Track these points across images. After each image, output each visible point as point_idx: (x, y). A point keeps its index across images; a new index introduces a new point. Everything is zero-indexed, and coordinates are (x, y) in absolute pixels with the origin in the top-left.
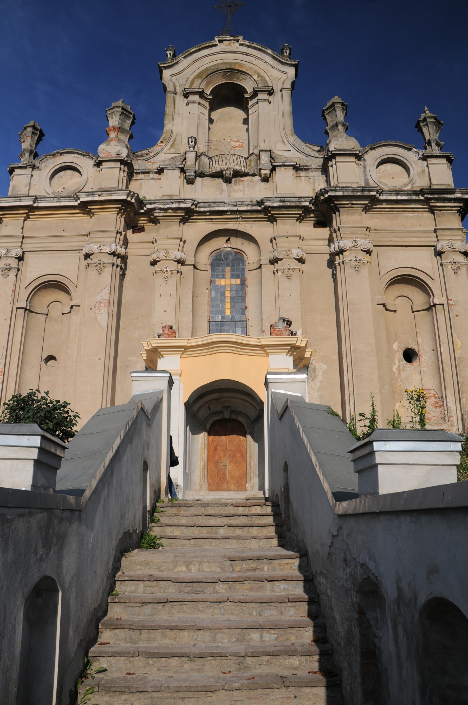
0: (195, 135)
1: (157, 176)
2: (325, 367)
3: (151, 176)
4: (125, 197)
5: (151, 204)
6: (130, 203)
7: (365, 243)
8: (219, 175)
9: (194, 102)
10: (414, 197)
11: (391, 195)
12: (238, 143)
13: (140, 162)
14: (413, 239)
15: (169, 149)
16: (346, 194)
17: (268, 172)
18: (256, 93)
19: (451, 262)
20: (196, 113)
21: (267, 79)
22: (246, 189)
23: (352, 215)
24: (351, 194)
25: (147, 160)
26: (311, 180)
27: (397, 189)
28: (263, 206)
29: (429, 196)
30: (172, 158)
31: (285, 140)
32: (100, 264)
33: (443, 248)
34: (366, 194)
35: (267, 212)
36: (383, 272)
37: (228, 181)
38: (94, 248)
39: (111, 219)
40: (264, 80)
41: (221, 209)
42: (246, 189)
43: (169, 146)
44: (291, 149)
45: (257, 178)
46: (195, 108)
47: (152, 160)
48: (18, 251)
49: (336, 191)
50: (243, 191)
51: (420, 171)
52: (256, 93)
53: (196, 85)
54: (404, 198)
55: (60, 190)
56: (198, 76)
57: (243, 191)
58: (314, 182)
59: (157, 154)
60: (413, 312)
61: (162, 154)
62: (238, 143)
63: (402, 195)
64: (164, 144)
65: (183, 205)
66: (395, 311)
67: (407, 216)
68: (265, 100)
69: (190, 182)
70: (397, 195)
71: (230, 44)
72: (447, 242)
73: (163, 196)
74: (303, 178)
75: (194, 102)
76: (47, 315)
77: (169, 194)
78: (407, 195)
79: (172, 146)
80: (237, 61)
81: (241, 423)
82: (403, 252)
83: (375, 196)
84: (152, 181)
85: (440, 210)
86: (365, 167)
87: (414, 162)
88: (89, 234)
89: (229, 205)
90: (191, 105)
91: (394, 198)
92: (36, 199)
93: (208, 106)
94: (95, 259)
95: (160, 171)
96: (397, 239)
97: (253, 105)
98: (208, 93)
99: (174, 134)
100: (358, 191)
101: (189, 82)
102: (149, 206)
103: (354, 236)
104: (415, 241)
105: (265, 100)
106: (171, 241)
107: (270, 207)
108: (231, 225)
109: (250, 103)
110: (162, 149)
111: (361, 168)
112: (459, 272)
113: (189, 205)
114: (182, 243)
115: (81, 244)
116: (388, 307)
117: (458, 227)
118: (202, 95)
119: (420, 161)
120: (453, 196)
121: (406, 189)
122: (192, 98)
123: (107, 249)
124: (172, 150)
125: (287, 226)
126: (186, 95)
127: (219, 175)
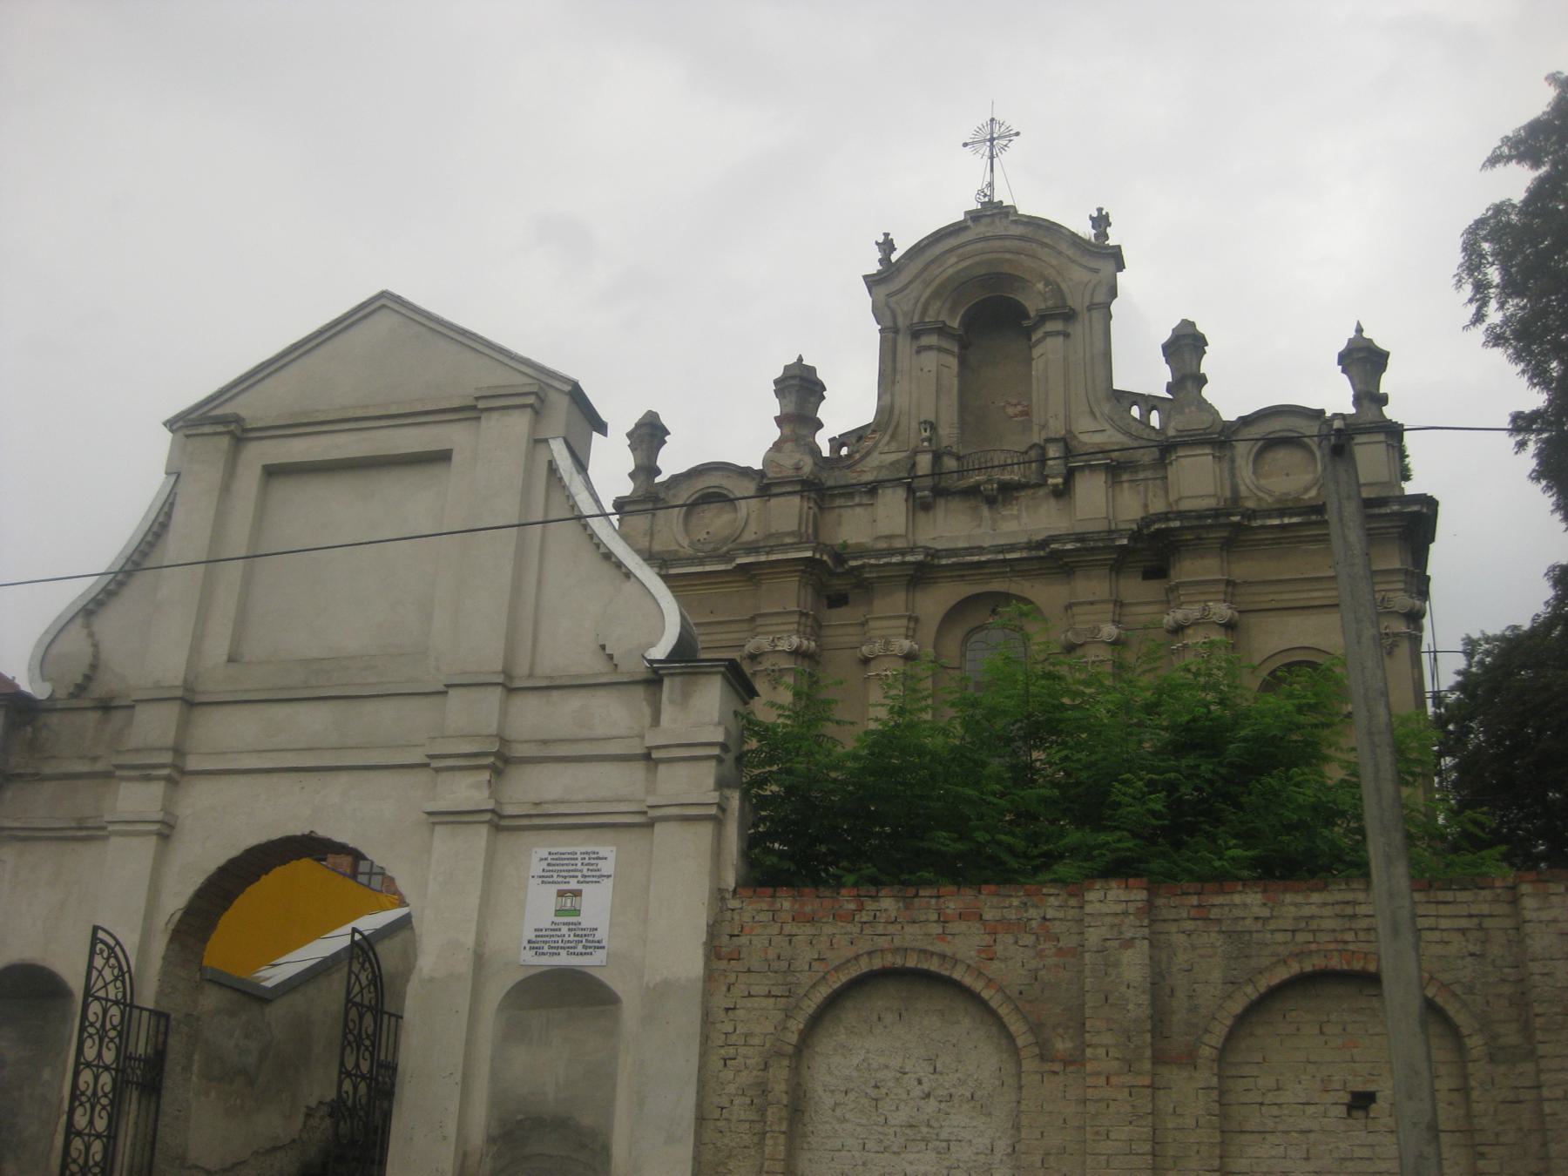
0: (932, 418)
1: (865, 500)
3: (857, 500)
4: (809, 554)
5: (855, 558)
7: (1221, 611)
8: (972, 492)
9: (930, 348)
10: (1314, 518)
12: (1020, 408)
13: (837, 473)
14: (1316, 594)
15: (888, 443)
17: (1060, 480)
18: (1044, 318)
20: (934, 369)
21: (1064, 286)
22: (1024, 514)
24: (1195, 523)
25: (849, 467)
26: (1141, 488)
30: (892, 464)
31: (1096, 410)
34: (1222, 520)
35: (1054, 560)
37: (991, 501)
38: (763, 642)
39: (788, 595)
40: (1058, 292)
41: (976, 558)
42: (1024, 514)
43: (887, 438)
44: (1106, 426)
45: (1042, 492)
46: (930, 360)
47: (859, 468)
49: (1168, 520)
50: (1018, 517)
52: (1044, 318)
53: (931, 312)
54: (1295, 520)
55: (702, 536)
56: (936, 294)
57: (1018, 517)
58: (1146, 491)
59: (868, 454)
61: (875, 454)
62: (1020, 408)
63: (1291, 516)
64: (877, 436)
65: (909, 558)
68: (1058, 333)
69: (926, 507)
71: (993, 222)
73: (878, 538)
74: (1126, 485)
75: (930, 348)
77: (887, 533)
79: (893, 437)
80: (1008, 256)
83: (1238, 524)
84: (859, 510)
86: (1233, 460)
88: (753, 619)
89: (990, 552)
90: (924, 355)
91: (1276, 522)
93: (956, 350)
94: (766, 664)
95: (873, 489)
96: (1286, 596)
97: (1039, 341)
98: (955, 324)
99: (896, 412)
100: (1208, 517)
101: (919, 305)
102: (853, 563)
105: (1058, 333)
106: (893, 623)
108: (996, 586)
110: (876, 445)
111: (1226, 466)
113: (920, 557)
114: (912, 625)
115: (741, 635)
117: (1397, 564)
118: (942, 330)
120: (1383, 511)
122: (926, 340)
123: (783, 645)
124: (894, 446)
125: (1091, 586)
126: (916, 335)
127: (972, 492)
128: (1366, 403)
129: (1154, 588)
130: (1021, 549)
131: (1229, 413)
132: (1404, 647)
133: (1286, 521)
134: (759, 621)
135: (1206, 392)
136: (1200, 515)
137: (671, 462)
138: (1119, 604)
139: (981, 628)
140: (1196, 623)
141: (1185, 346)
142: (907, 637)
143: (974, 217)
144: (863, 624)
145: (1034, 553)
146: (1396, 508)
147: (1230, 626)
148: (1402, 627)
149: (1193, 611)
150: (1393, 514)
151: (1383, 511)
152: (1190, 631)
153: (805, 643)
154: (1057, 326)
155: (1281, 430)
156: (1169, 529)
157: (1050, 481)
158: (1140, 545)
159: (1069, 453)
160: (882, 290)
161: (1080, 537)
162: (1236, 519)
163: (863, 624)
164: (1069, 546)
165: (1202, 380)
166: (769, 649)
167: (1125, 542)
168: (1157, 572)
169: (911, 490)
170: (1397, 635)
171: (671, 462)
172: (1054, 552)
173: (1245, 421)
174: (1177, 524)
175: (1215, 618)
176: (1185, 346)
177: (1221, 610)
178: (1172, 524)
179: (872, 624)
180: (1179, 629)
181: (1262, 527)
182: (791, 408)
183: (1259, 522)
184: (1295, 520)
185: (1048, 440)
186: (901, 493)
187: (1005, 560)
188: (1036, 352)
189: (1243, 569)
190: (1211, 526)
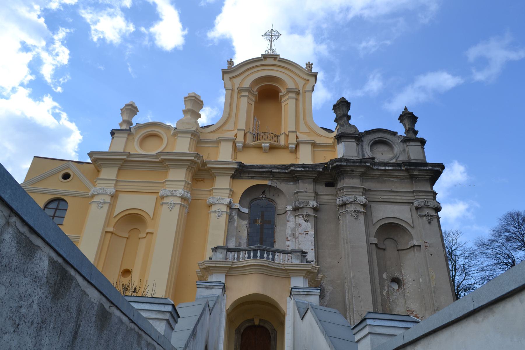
2: (332, 288)
4: (193, 158)
6: (196, 163)
11: (381, 166)
16: (348, 164)
17: (294, 146)
19: (425, 215)
23: (353, 179)
24: (352, 164)
27: (385, 161)
28: (289, 170)
29: (409, 167)
32: (171, 203)
33: (419, 205)
34: (363, 164)
36: (375, 221)
48: (112, 190)
49: (342, 162)
51: (401, 150)
54: (390, 168)
60: (398, 250)
63: (389, 167)
66: (384, 249)
67: (393, 181)
70: (385, 166)
72: (423, 200)
76: (127, 238)
78: (392, 166)
81: (267, 330)
82: (389, 207)
83: (369, 166)
85: (417, 178)
86: (362, 146)
87: (397, 143)
91: (383, 168)
92: (129, 155)
103: (354, 193)
104: (398, 198)
107: (294, 170)
109: (283, 99)
111: (360, 147)
112: (432, 222)
116: (378, 246)
119: (401, 144)
120: (425, 168)
121: (392, 162)
122: (243, 94)
128: (411, 132)
129: (330, 190)
130: (279, 168)
131: (361, 130)
132: (435, 220)
133: (387, 168)
134: (167, 183)
135: (351, 122)
136: (354, 162)
137: (137, 120)
138: (316, 194)
139: (257, 199)
140: (351, 203)
141: (342, 107)
142: (229, 197)
143: (265, 57)
144: (210, 191)
145: (283, 171)
146: (430, 168)
147: (364, 206)
148: (433, 213)
149: (351, 199)
150: (429, 170)
151: (425, 168)
152: (348, 206)
153: (186, 194)
154: (294, 95)
155: (380, 138)
156: (341, 166)
157: (290, 146)
158: (326, 172)
159: (297, 137)
160: (227, 77)
161: (303, 166)
162: (369, 164)
163: (210, 191)
164: (298, 169)
165: (349, 118)
166: (170, 194)
167: (321, 170)
168: (330, 184)
169: (234, 143)
170: (432, 216)
171: (137, 120)
172: (292, 171)
173: (367, 133)
174: (345, 164)
175: (359, 202)
176: (342, 107)
177: (362, 199)
178: (343, 164)
179: (214, 191)
180: (344, 204)
181: (377, 169)
182: (190, 107)
183: (376, 167)
184: (390, 168)
185: (289, 132)
186: (230, 145)
187: (272, 172)
188: (283, 104)
189: (368, 185)
190: (358, 166)
